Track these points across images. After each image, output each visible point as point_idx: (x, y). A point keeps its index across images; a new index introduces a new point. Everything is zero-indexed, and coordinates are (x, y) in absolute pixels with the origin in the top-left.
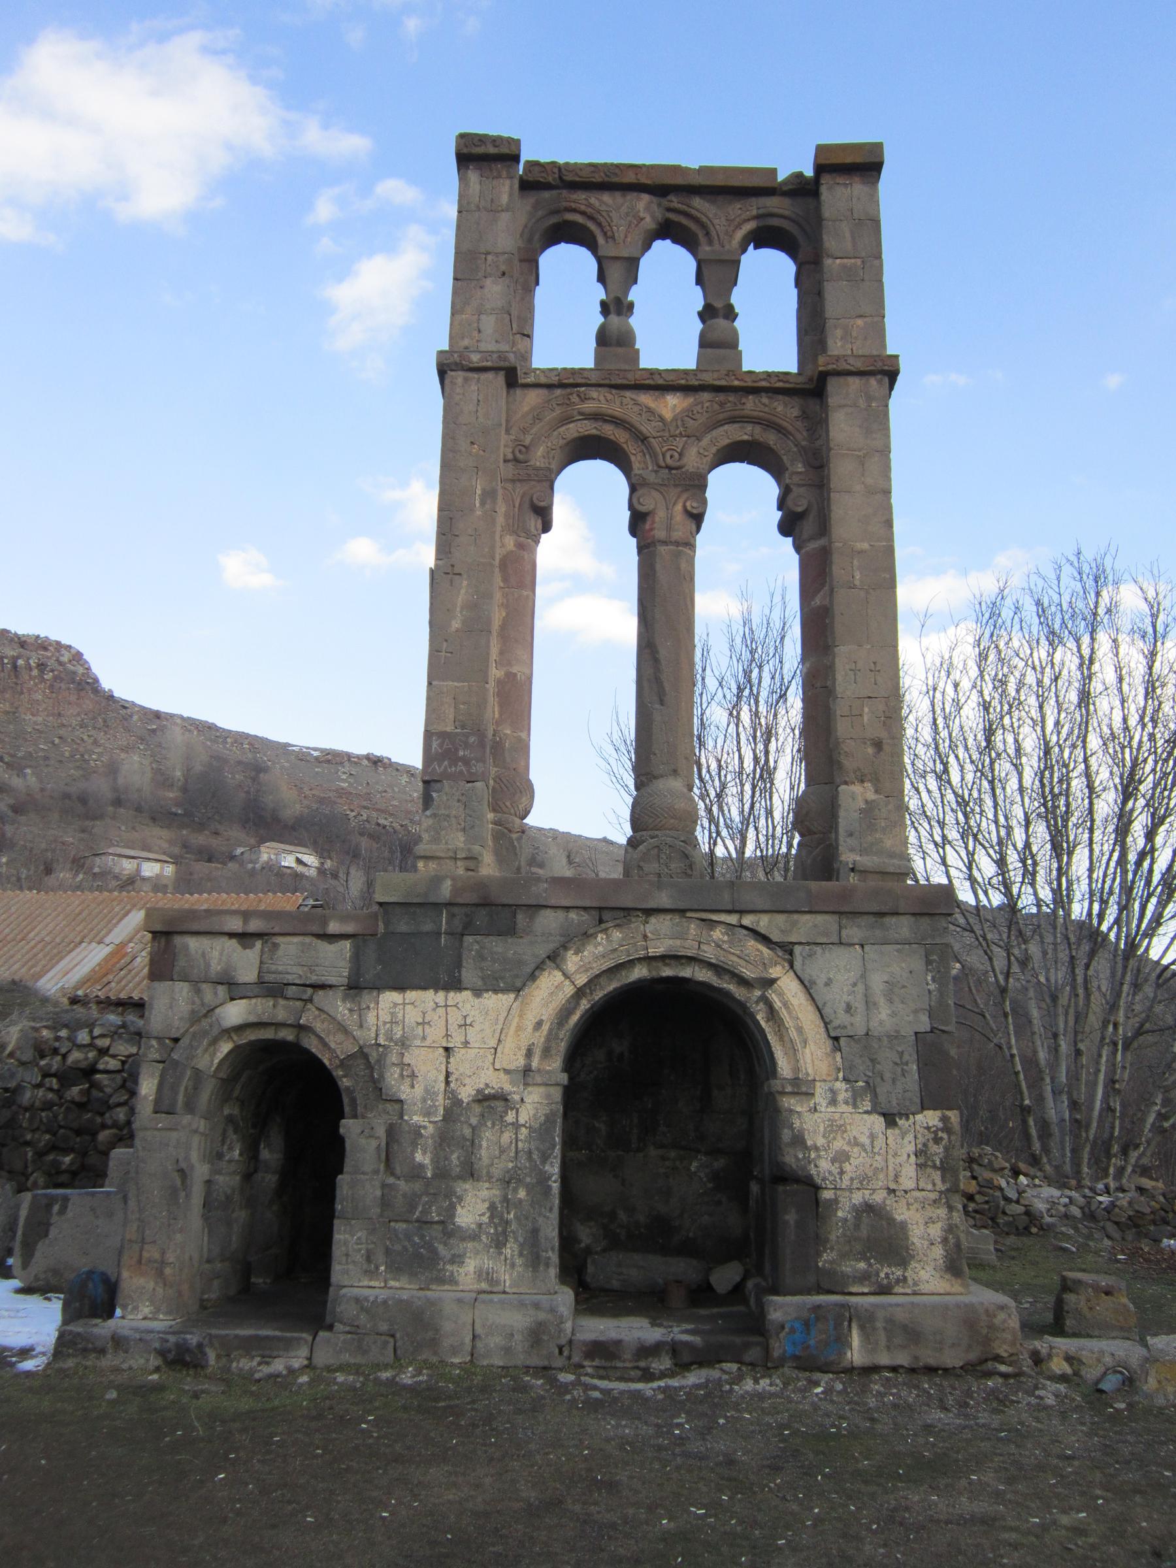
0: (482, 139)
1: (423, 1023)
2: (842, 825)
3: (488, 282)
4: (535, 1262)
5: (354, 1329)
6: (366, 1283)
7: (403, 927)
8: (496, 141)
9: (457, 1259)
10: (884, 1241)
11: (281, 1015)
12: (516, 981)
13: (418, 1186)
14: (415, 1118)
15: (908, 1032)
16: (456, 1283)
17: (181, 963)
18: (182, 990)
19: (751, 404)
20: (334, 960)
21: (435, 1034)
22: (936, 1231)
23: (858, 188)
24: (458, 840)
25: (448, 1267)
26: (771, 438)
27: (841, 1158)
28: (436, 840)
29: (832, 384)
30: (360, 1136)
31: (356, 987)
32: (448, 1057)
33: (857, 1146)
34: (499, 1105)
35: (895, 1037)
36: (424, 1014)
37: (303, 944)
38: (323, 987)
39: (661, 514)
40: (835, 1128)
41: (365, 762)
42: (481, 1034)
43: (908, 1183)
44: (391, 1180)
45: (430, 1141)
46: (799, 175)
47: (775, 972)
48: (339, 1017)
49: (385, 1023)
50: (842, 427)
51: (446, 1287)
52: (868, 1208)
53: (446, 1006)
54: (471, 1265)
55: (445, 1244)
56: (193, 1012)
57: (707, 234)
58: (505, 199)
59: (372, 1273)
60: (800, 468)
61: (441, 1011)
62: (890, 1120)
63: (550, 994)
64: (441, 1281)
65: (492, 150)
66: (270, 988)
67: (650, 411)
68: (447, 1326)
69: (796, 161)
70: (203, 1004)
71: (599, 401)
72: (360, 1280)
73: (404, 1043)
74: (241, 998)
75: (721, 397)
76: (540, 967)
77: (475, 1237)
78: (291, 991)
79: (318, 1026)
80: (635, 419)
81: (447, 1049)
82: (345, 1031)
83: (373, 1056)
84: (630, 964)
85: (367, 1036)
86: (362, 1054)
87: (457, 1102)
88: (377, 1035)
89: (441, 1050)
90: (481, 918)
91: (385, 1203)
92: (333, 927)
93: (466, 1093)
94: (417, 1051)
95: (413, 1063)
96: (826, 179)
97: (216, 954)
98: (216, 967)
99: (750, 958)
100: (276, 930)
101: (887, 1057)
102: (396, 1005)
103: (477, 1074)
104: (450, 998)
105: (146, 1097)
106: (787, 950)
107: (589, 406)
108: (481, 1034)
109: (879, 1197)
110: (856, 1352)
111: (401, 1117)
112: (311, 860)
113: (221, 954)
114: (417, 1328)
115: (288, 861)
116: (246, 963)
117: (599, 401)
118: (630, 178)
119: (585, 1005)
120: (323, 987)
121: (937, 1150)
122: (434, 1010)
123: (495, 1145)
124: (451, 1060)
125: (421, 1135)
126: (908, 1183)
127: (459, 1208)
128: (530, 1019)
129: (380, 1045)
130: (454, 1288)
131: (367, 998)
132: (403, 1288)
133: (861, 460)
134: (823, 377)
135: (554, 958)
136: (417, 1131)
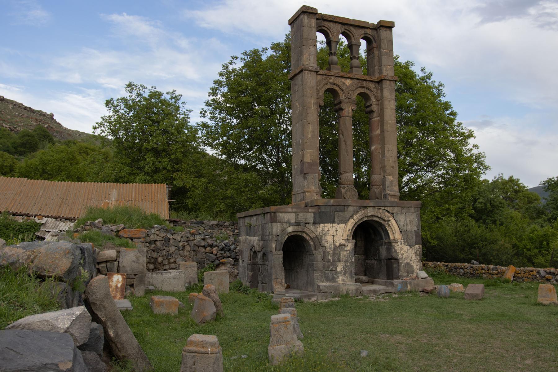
0: (309, 8)
2: (387, 185)
3: (311, 47)
7: (323, 210)
8: (312, 8)
9: (338, 277)
10: (409, 269)
11: (300, 230)
12: (346, 222)
13: (330, 263)
15: (413, 230)
17: (278, 219)
19: (365, 84)
20: (310, 217)
21: (331, 233)
22: (418, 267)
23: (388, 32)
26: (368, 92)
27: (403, 254)
28: (308, 187)
31: (315, 223)
34: (343, 247)
35: (411, 231)
39: (347, 110)
42: (340, 232)
43: (413, 259)
46: (374, 24)
47: (391, 219)
52: (407, 264)
54: (340, 278)
58: (314, 24)
59: (322, 281)
62: (411, 247)
63: (351, 224)
64: (335, 282)
65: (312, 11)
66: (298, 224)
67: (344, 83)
69: (374, 21)
71: (334, 80)
73: (325, 235)
75: (359, 81)
76: (349, 218)
77: (341, 273)
79: (307, 232)
80: (341, 85)
83: (319, 238)
84: (363, 218)
85: (318, 233)
86: (317, 237)
87: (335, 246)
91: (324, 267)
92: (310, 210)
93: (337, 244)
96: (381, 28)
98: (286, 220)
103: (340, 240)
106: (393, 214)
107: (331, 81)
108: (340, 232)
109: (409, 261)
117: (334, 80)
118: (338, 21)
119: (356, 226)
121: (418, 252)
123: (343, 254)
131: (317, 225)
132: (328, 284)
133: (390, 101)
134: (382, 80)
135: (352, 217)
136: (329, 252)
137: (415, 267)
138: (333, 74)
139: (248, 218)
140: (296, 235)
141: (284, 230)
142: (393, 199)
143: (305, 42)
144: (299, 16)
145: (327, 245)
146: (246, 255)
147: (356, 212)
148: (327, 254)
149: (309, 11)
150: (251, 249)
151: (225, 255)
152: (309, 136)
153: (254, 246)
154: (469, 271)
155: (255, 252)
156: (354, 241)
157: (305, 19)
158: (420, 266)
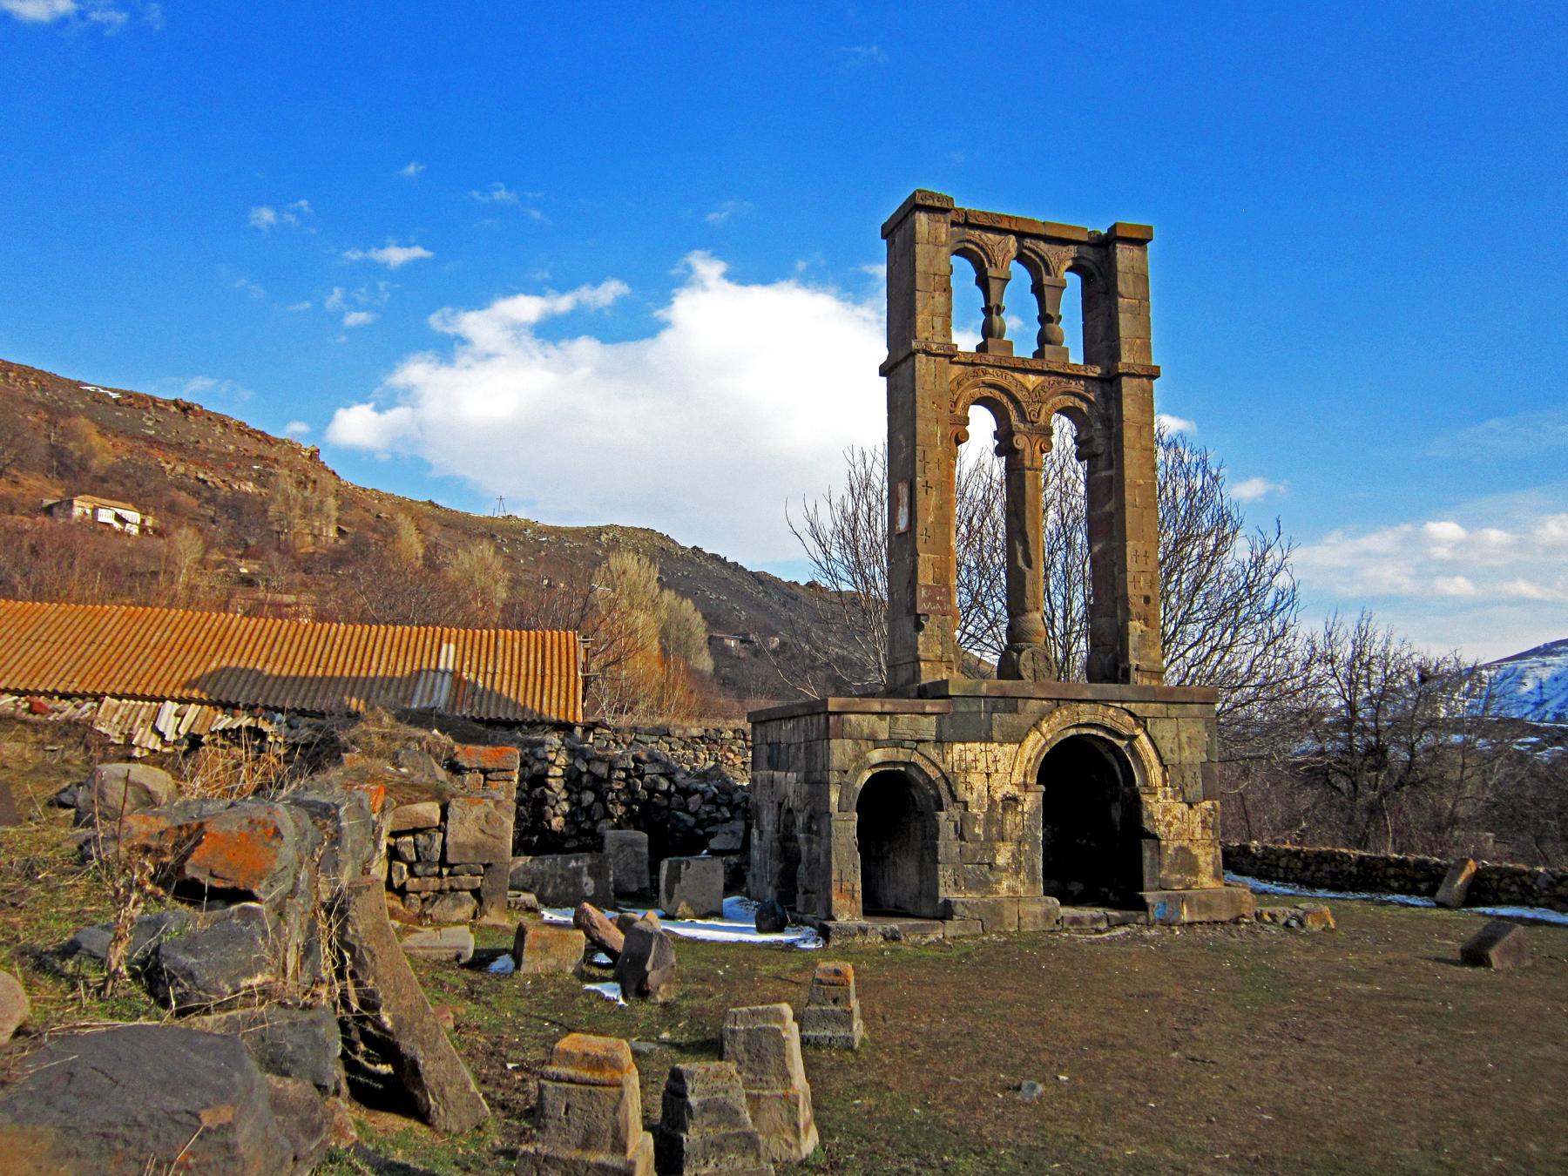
4: (1034, 881)
5: (963, 918)
7: (962, 709)
8: (940, 198)
9: (999, 882)
10: (1188, 863)
11: (901, 757)
13: (977, 846)
15: (1197, 762)
18: (849, 743)
19: (1074, 386)
21: (981, 765)
22: (1210, 859)
23: (1136, 251)
24: (938, 650)
27: (1169, 824)
28: (927, 649)
29: (1124, 380)
30: (946, 819)
33: (1176, 819)
39: (1028, 451)
40: (1166, 810)
41: (173, 409)
43: (1198, 836)
50: (1129, 409)
52: (1181, 849)
54: (1005, 884)
57: (1047, 266)
59: (958, 890)
60: (1099, 426)
62: (1191, 806)
63: (1035, 745)
64: (991, 893)
65: (938, 204)
68: (1006, 913)
73: (967, 771)
77: (1006, 870)
78: (907, 744)
79: (922, 763)
80: (1013, 390)
82: (934, 764)
87: (993, 802)
90: (1001, 704)
92: (928, 709)
93: (998, 796)
98: (866, 731)
99: (1126, 724)
101: (1188, 774)
106: (1141, 721)
107: (987, 378)
109: (1186, 843)
110: (1185, 916)
112: (133, 516)
114: (994, 912)
115: (106, 516)
116: (882, 729)
117: (992, 376)
118: (1005, 225)
126: (1198, 836)
128: (1026, 757)
132: (973, 896)
135: (1036, 726)
136: (975, 817)
137: (1201, 860)
138: (991, 360)
139: (774, 724)
141: (859, 756)
142: (1146, 682)
143: (920, 283)
144: (906, 216)
146: (768, 818)
147: (1045, 714)
148: (970, 821)
149: (929, 202)
150: (780, 805)
151: (718, 815)
152: (931, 519)
153: (786, 796)
154: (1354, 870)
155: (790, 811)
156: (1042, 787)
157: (922, 220)
158: (1215, 857)
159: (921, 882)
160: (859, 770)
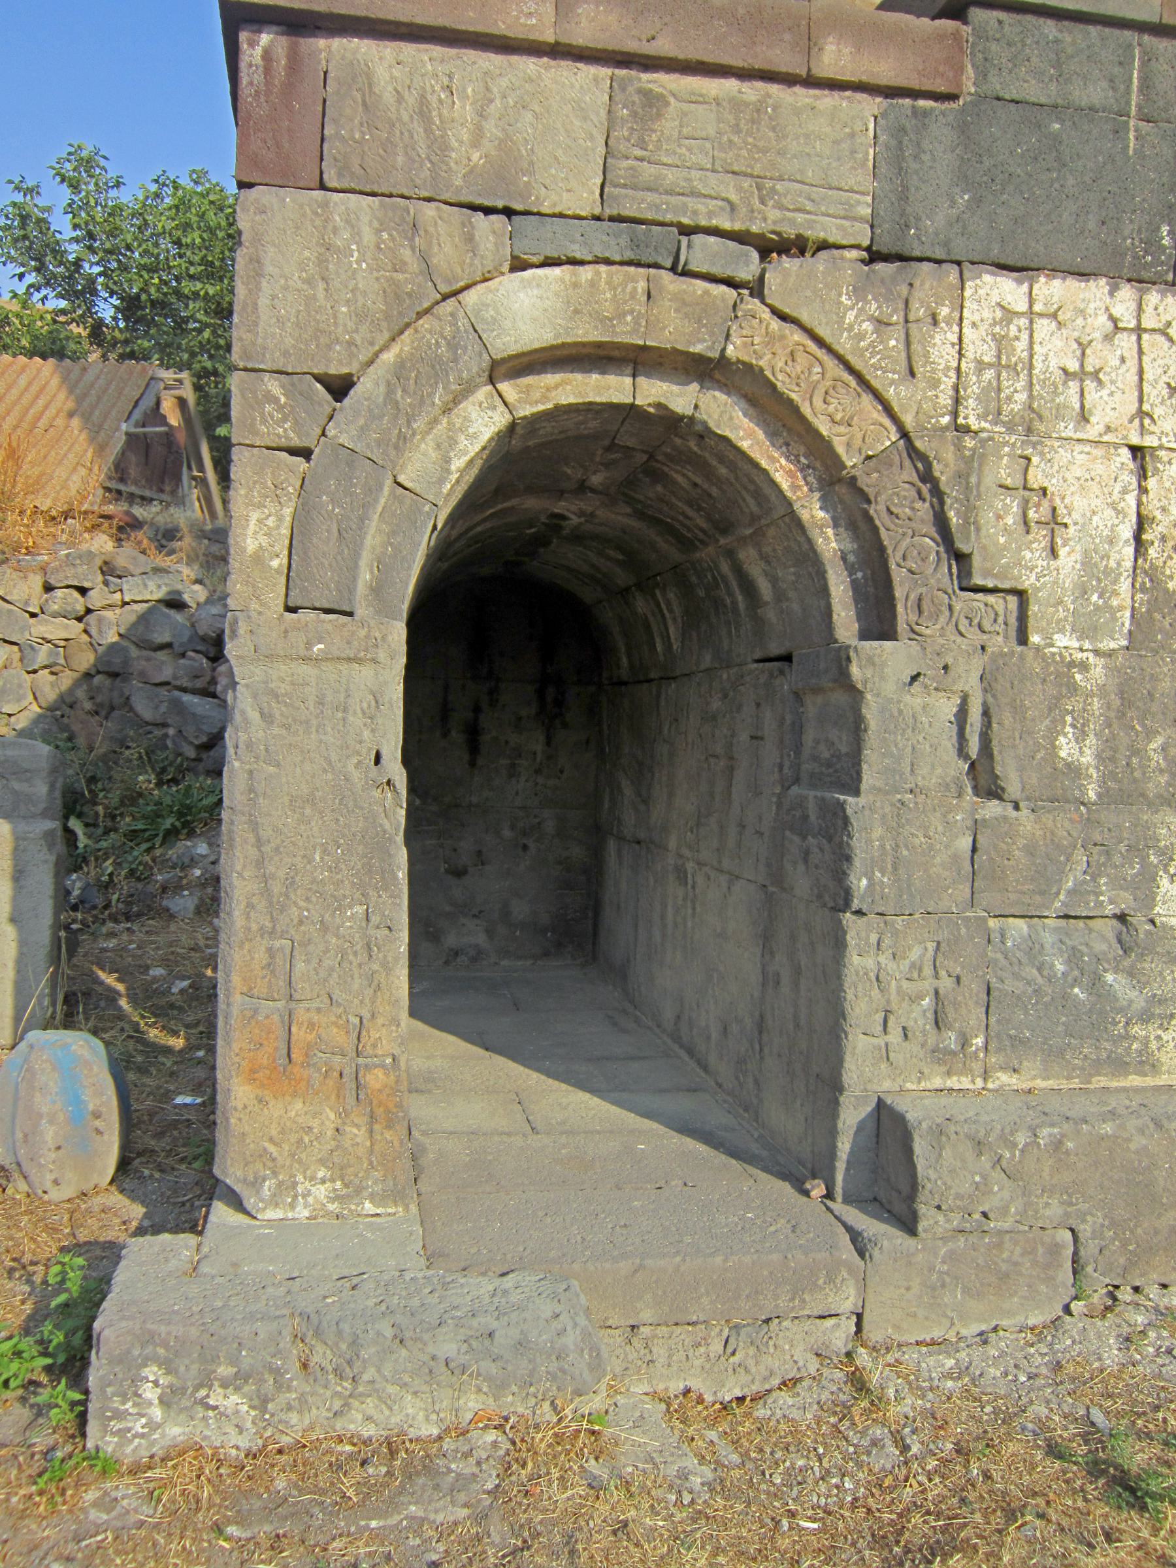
1: (1081, 375)
6: (937, 1082)
11: (672, 330)
13: (1063, 824)
14: (1062, 641)
16: (1155, 1068)
17: (346, 129)
21: (1111, 406)
25: (1136, 1030)
32: (1142, 474)
36: (1083, 347)
37: (737, 105)
38: (797, 247)
44: (993, 809)
45: (1096, 704)
48: (844, 344)
49: (981, 366)
51: (1134, 1080)
53: (1139, 330)
55: (1131, 974)
56: (394, 294)
61: (1126, 342)
64: (1120, 1066)
70: (429, 271)
72: (922, 1076)
74: (549, 263)
78: (703, 253)
81: (1135, 450)
88: (957, 401)
89: (1125, 453)
92: (834, 58)
94: (1063, 456)
95: (1052, 485)
97: (463, 110)
100: (664, 47)
102: (1009, 314)
104: (1149, 310)
105: (258, 558)
111: (1023, 640)
113: (481, 114)
120: (797, 247)
122: (1108, 338)
124: (1151, 483)
125: (1074, 688)
127: (1164, 882)
129: (966, 430)
130: (1149, 1081)
140: (630, 411)
145: (1049, 574)
159: (770, 980)
160: (431, 383)
